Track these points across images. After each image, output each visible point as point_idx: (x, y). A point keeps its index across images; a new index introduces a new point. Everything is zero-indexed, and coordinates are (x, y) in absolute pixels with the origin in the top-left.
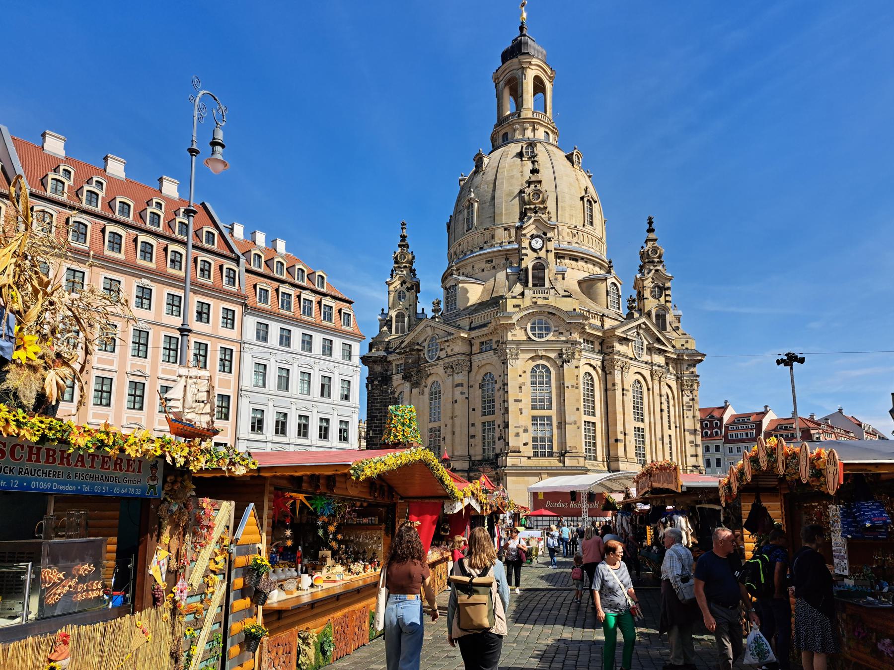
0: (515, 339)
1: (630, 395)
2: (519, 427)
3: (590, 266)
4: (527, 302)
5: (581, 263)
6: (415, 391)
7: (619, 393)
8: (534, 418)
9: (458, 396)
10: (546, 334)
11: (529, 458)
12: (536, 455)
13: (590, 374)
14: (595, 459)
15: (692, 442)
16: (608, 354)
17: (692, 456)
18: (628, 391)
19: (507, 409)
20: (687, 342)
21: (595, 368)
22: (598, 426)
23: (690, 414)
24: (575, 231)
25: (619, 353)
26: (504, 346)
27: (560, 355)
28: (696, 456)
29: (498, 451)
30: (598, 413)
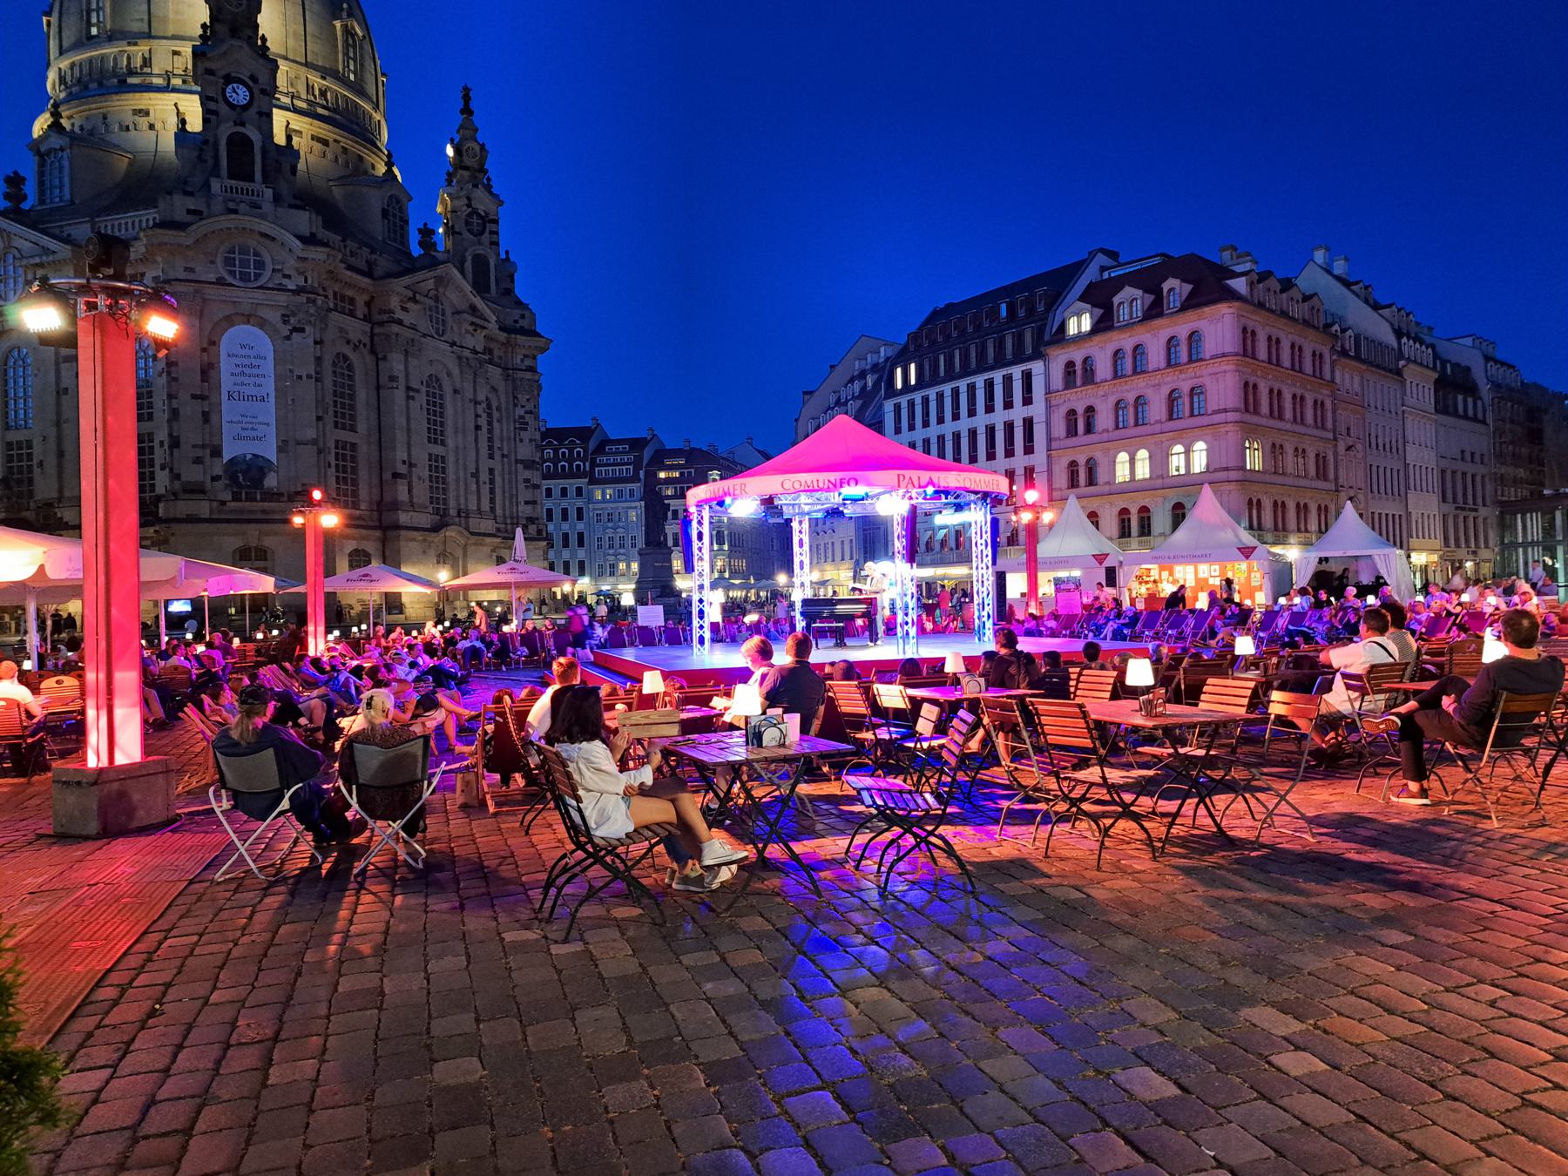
0: (191, 277)
1: (422, 398)
2: (203, 446)
4: (217, 206)
7: (400, 395)
10: (257, 276)
11: (223, 503)
13: (346, 358)
15: (527, 481)
16: (381, 324)
18: (417, 391)
21: (356, 347)
22: (363, 449)
23: (525, 435)
25: (400, 322)
27: (285, 319)
28: (534, 503)
29: (160, 490)
30: (362, 427)
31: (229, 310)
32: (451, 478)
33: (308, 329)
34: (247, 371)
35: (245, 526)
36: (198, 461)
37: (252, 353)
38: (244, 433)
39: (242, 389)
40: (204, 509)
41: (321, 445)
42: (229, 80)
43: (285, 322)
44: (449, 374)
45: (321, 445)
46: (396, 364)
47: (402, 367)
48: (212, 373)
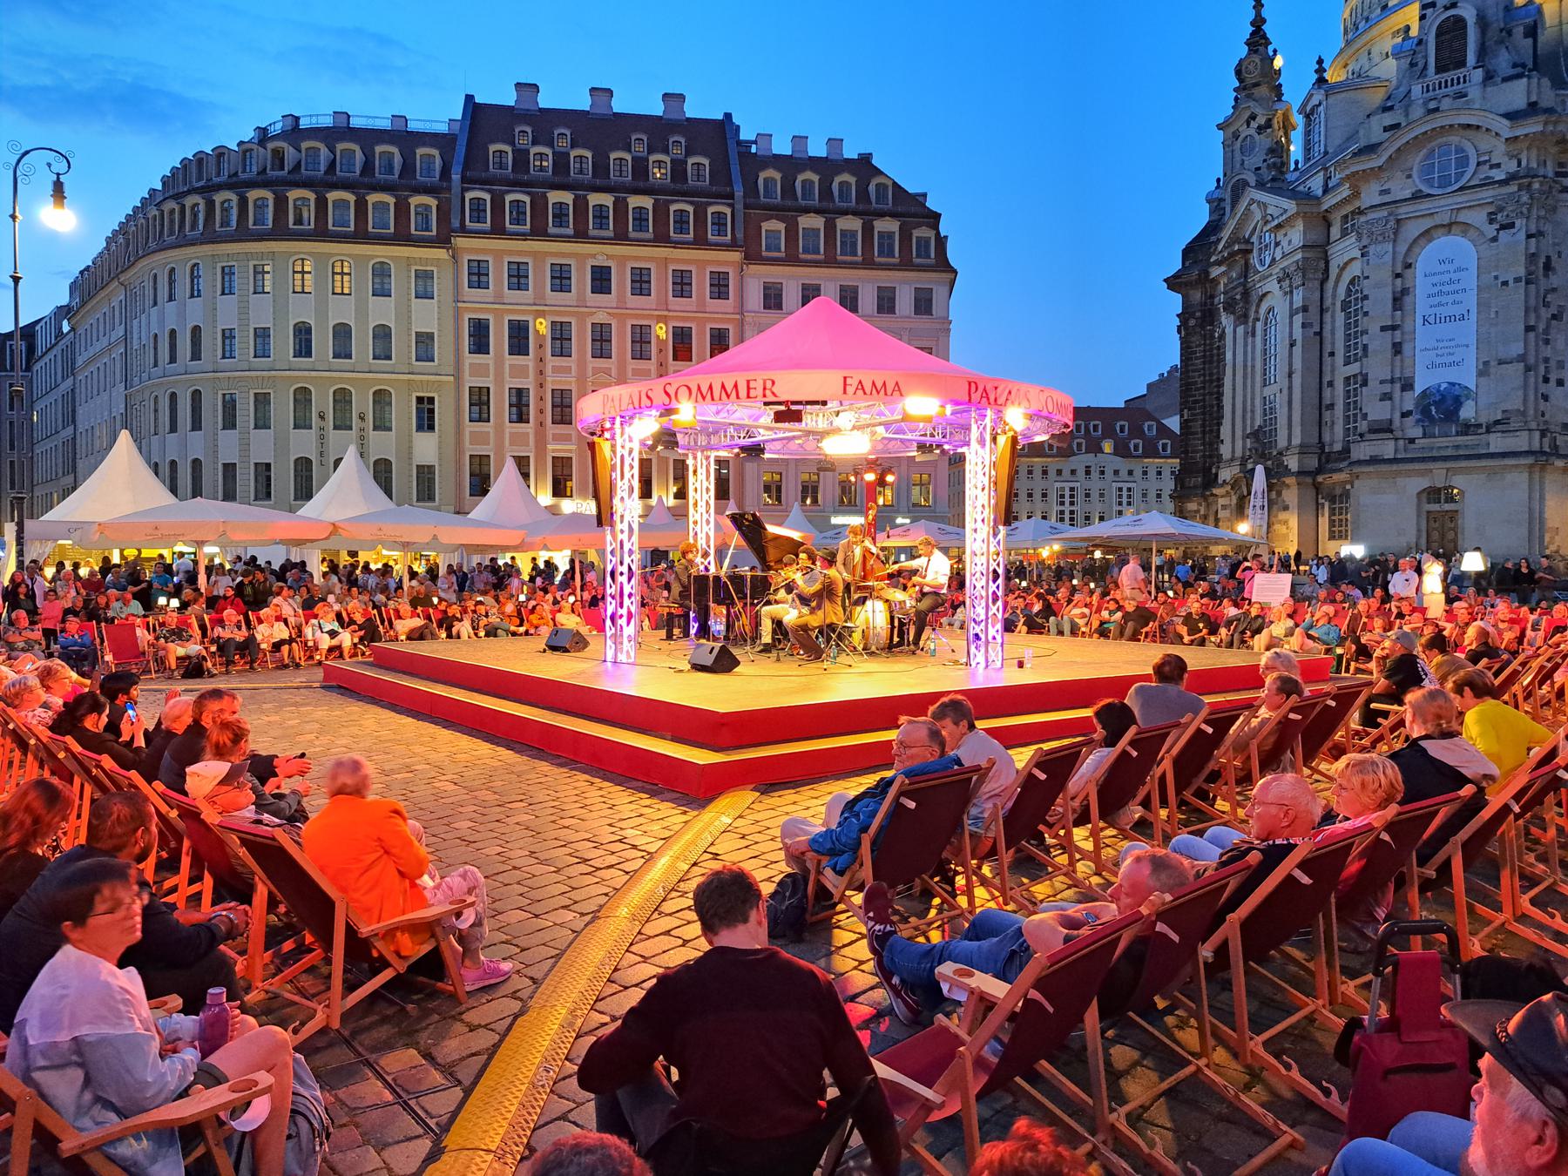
0: (1387, 198)
4: (1417, 112)
6: (1241, 330)
9: (1298, 333)
10: (1459, 176)
11: (1412, 441)
19: (1365, 347)
26: (1363, 219)
31: (1427, 223)
33: (1518, 223)
34: (1446, 288)
35: (1431, 465)
36: (1386, 397)
37: (1451, 267)
38: (1439, 360)
39: (1438, 310)
40: (1388, 449)
41: (1531, 360)
43: (1491, 221)
45: (1531, 360)
48: (1407, 299)
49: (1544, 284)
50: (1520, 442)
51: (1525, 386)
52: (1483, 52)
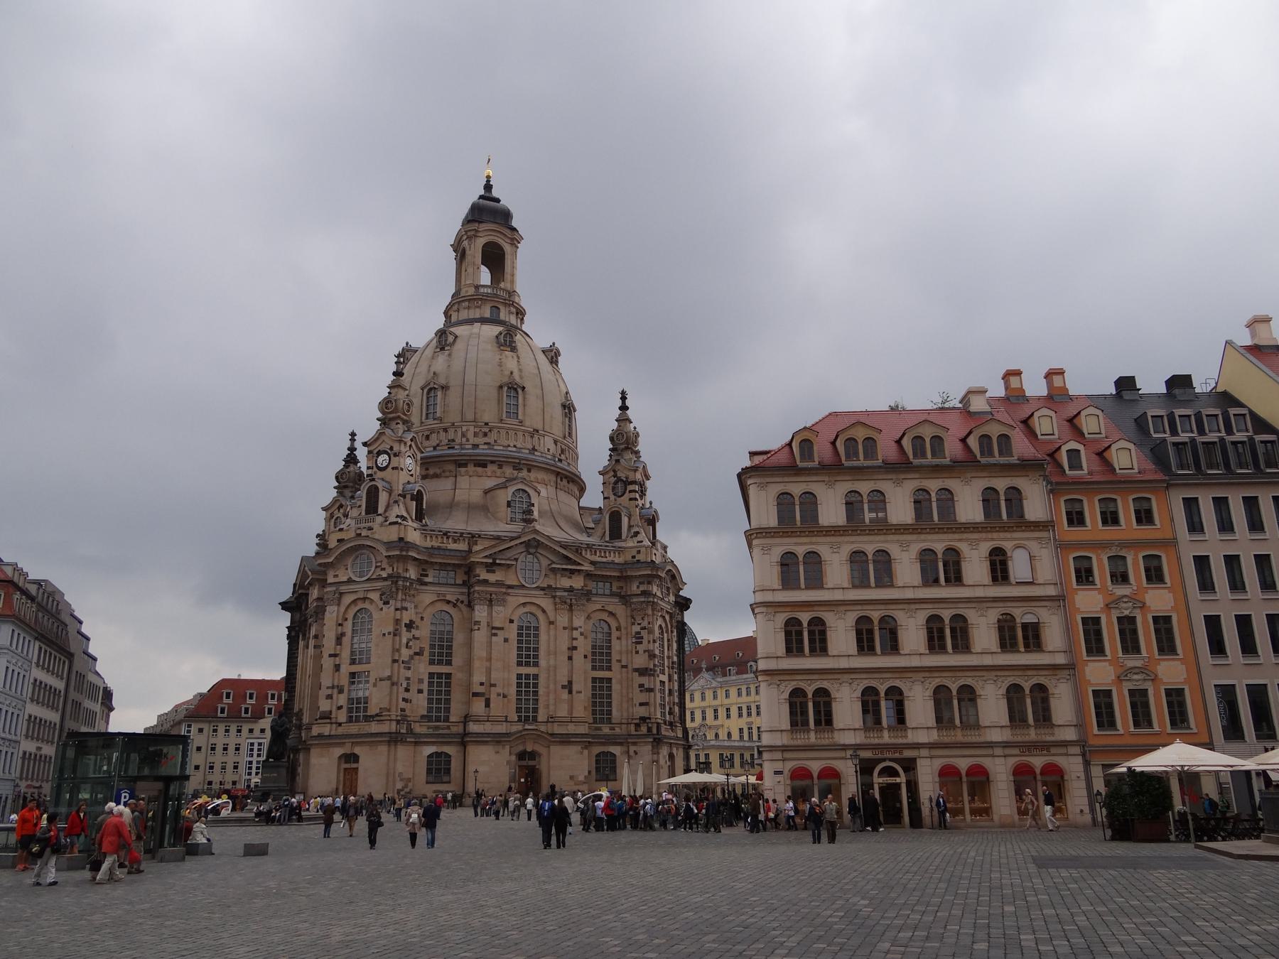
0: (336, 580)
1: (512, 632)
3: (509, 471)
4: (353, 535)
5: (491, 468)
8: (353, 675)
11: (340, 724)
12: (350, 720)
14: (447, 719)
15: (641, 686)
17: (641, 704)
18: (502, 629)
20: (639, 552)
21: (455, 605)
22: (458, 677)
23: (640, 648)
24: (486, 429)
25: (486, 582)
30: (457, 660)
32: (541, 690)
36: (329, 697)
41: (395, 679)
42: (379, 453)
44: (544, 611)
45: (395, 679)
46: (481, 612)
47: (485, 614)
49: (405, 636)
50: (385, 728)
51: (391, 694)
52: (388, 507)
